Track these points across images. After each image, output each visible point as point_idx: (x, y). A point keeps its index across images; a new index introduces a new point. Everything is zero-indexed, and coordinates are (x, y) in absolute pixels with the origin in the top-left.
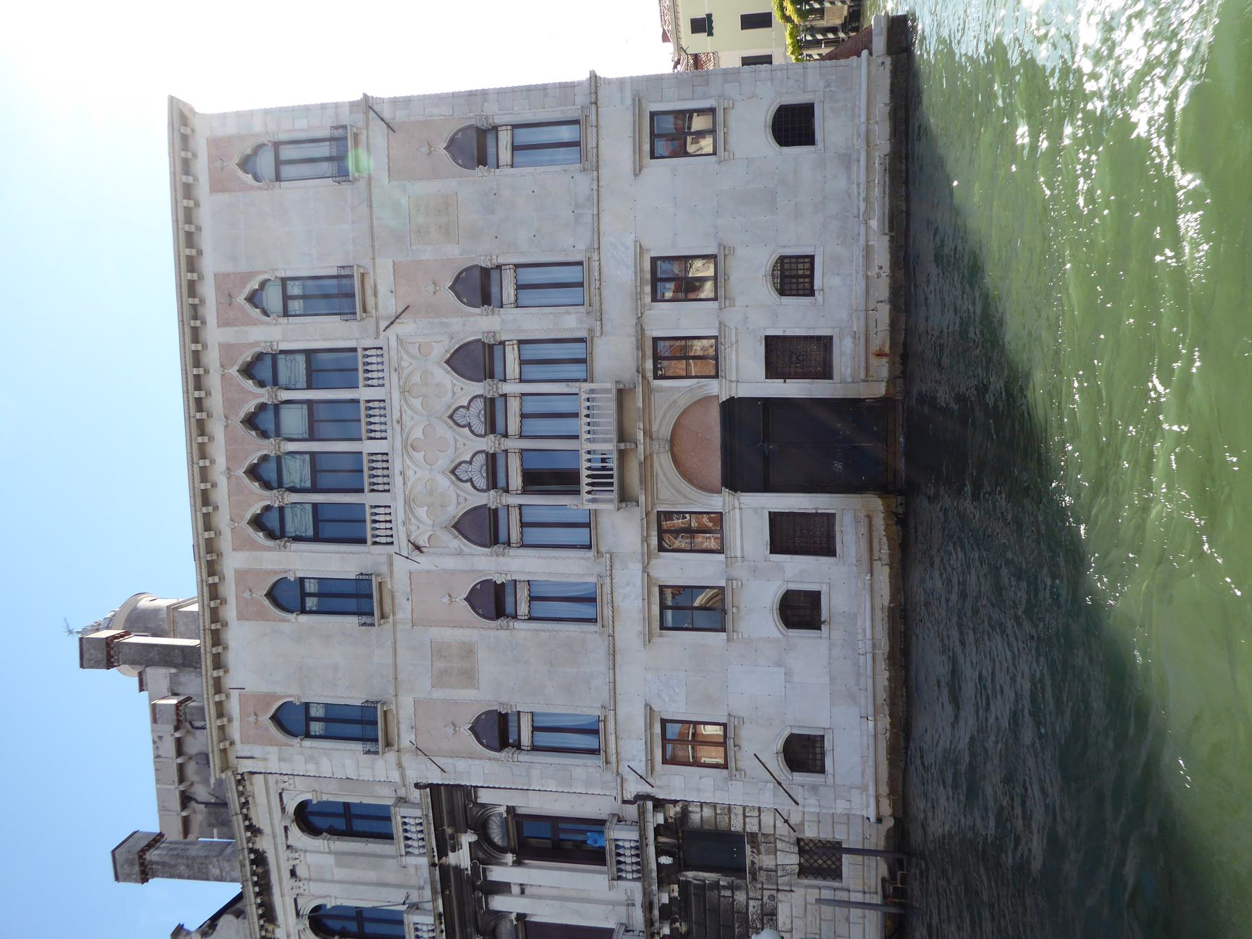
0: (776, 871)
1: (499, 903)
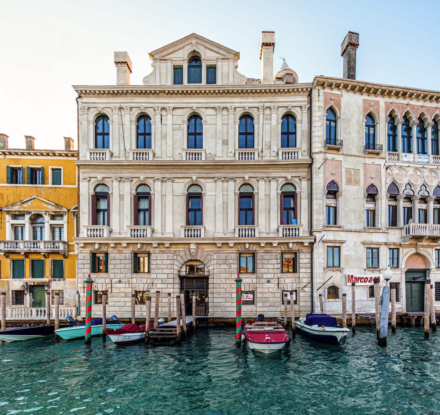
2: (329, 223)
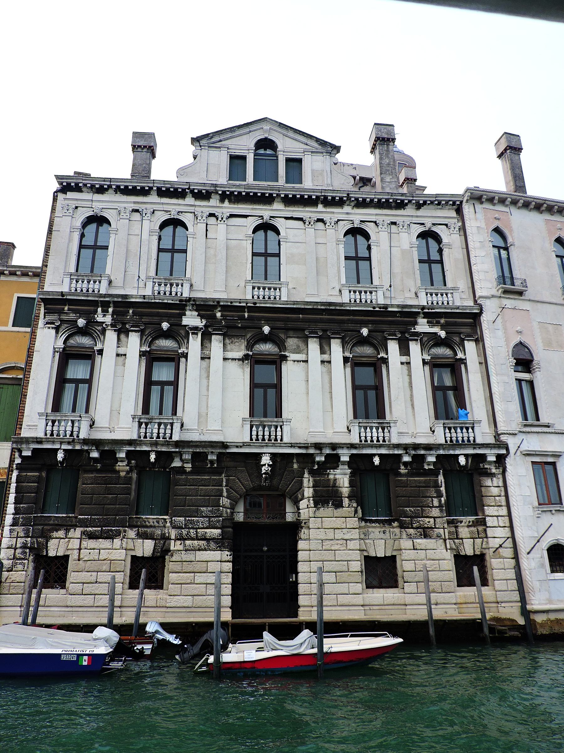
0: (457, 538)
1: (393, 347)
2: (526, 419)
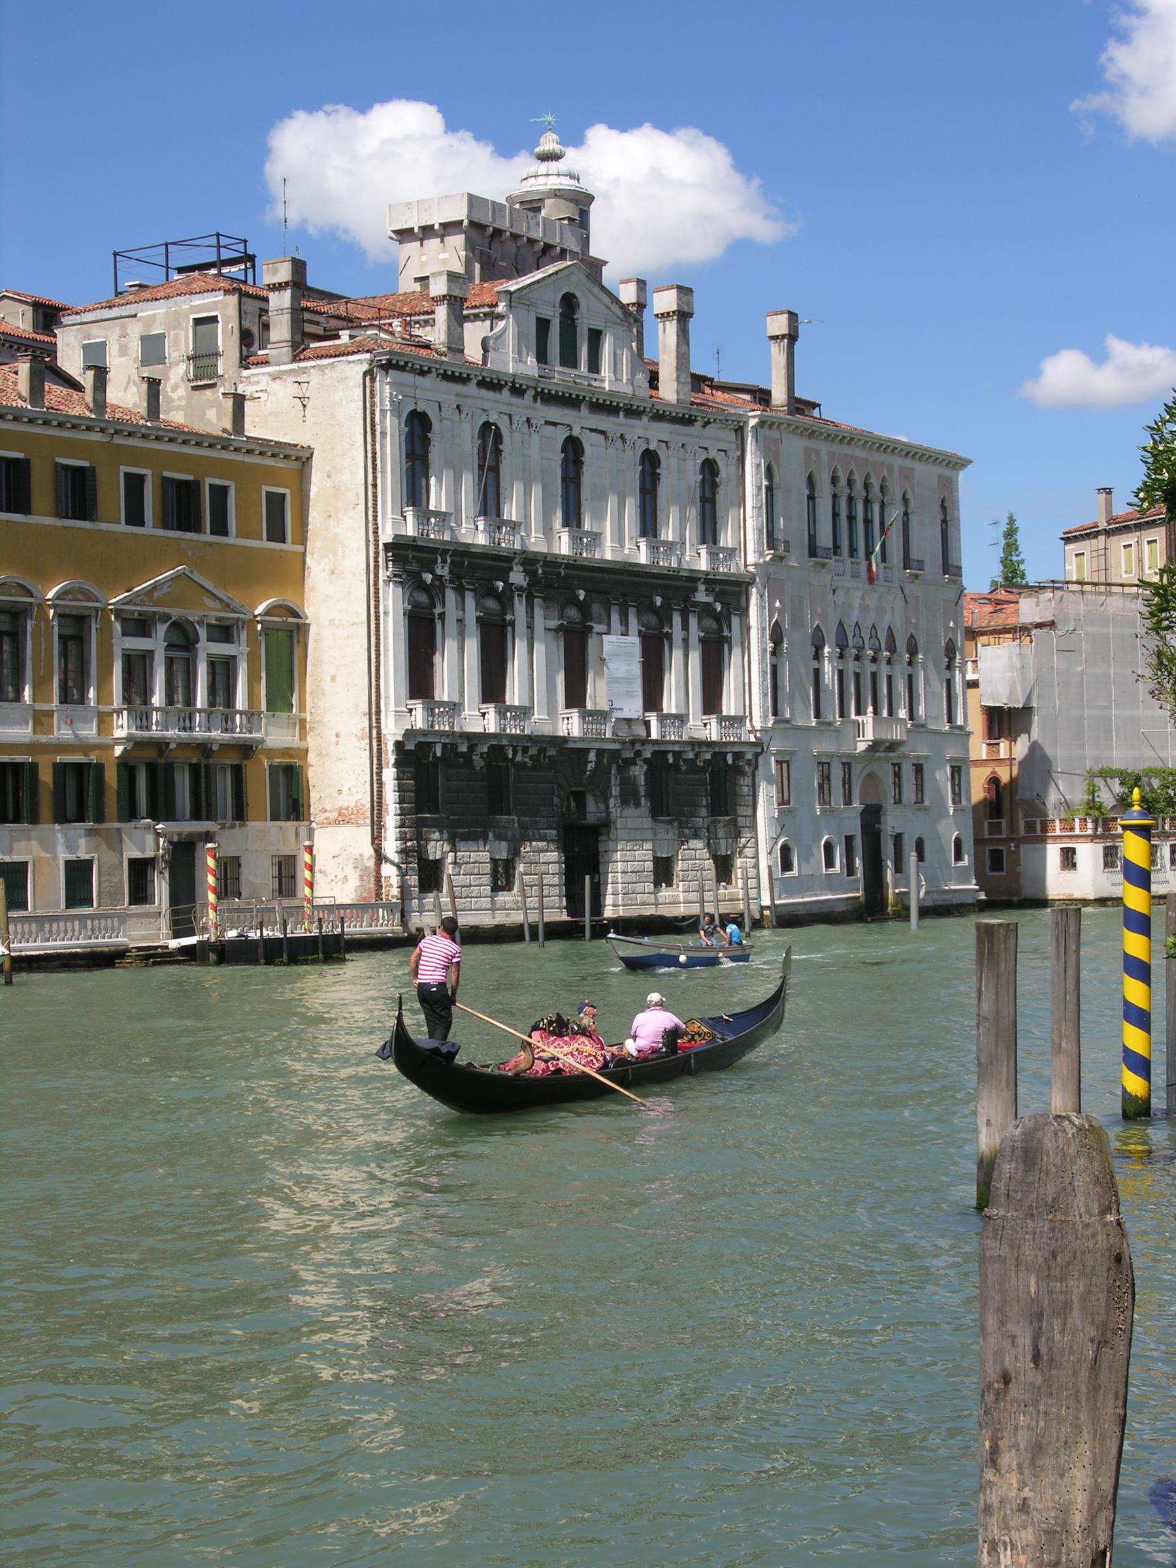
1: (677, 620)
